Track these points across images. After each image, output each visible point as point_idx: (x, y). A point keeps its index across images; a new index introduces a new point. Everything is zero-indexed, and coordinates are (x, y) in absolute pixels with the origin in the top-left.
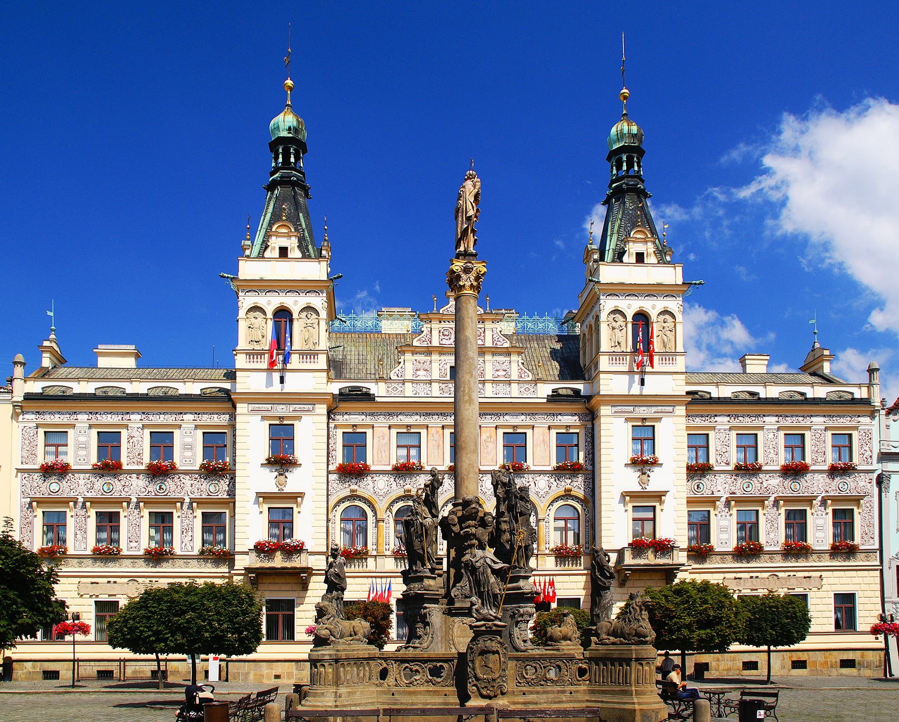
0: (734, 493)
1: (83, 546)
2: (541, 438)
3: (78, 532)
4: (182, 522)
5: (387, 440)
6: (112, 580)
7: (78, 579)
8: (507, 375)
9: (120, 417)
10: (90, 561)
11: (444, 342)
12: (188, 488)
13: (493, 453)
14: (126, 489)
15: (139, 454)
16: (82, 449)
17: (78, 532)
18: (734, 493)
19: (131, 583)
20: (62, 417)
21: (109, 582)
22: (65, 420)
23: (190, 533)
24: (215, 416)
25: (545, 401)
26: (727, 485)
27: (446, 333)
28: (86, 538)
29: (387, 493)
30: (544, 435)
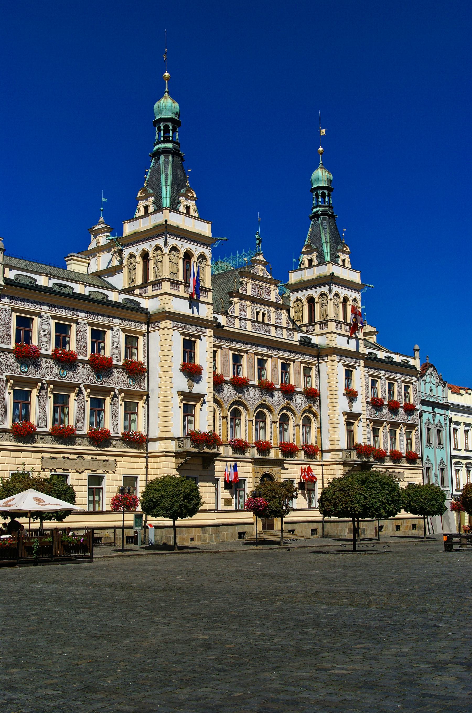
1: (44, 424)
2: (297, 369)
3: (41, 411)
4: (112, 409)
5: (227, 358)
6: (66, 456)
7: (40, 455)
8: (281, 323)
9: (71, 312)
10: (49, 438)
11: (253, 293)
12: (115, 380)
13: (277, 376)
14: (75, 376)
15: (84, 347)
16: (42, 336)
17: (41, 411)
19: (78, 459)
20: (30, 305)
21: (64, 458)
22: (32, 308)
23: (117, 418)
24: (133, 323)
25: (298, 344)
27: (254, 287)
28: (45, 416)
29: (229, 398)
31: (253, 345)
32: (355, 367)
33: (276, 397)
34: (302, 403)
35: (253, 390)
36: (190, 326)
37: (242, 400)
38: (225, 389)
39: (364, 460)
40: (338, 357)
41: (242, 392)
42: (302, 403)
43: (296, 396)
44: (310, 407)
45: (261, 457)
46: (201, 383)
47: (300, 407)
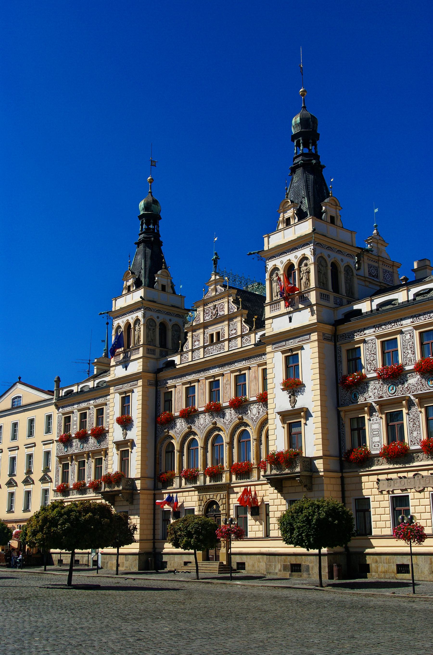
0: (381, 397)
2: (254, 375)
18: (381, 397)
26: (376, 391)
30: (255, 372)
31: (199, 372)
32: (302, 348)
33: (228, 416)
34: (259, 413)
35: (204, 416)
36: (126, 385)
37: (193, 430)
38: (227, 414)
39: (287, 471)
40: (274, 346)
41: (193, 422)
42: (259, 413)
43: (252, 407)
44: (215, 423)
45: (212, 483)
46: (133, 429)
47: (257, 418)
